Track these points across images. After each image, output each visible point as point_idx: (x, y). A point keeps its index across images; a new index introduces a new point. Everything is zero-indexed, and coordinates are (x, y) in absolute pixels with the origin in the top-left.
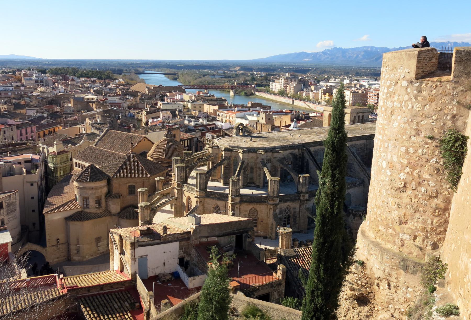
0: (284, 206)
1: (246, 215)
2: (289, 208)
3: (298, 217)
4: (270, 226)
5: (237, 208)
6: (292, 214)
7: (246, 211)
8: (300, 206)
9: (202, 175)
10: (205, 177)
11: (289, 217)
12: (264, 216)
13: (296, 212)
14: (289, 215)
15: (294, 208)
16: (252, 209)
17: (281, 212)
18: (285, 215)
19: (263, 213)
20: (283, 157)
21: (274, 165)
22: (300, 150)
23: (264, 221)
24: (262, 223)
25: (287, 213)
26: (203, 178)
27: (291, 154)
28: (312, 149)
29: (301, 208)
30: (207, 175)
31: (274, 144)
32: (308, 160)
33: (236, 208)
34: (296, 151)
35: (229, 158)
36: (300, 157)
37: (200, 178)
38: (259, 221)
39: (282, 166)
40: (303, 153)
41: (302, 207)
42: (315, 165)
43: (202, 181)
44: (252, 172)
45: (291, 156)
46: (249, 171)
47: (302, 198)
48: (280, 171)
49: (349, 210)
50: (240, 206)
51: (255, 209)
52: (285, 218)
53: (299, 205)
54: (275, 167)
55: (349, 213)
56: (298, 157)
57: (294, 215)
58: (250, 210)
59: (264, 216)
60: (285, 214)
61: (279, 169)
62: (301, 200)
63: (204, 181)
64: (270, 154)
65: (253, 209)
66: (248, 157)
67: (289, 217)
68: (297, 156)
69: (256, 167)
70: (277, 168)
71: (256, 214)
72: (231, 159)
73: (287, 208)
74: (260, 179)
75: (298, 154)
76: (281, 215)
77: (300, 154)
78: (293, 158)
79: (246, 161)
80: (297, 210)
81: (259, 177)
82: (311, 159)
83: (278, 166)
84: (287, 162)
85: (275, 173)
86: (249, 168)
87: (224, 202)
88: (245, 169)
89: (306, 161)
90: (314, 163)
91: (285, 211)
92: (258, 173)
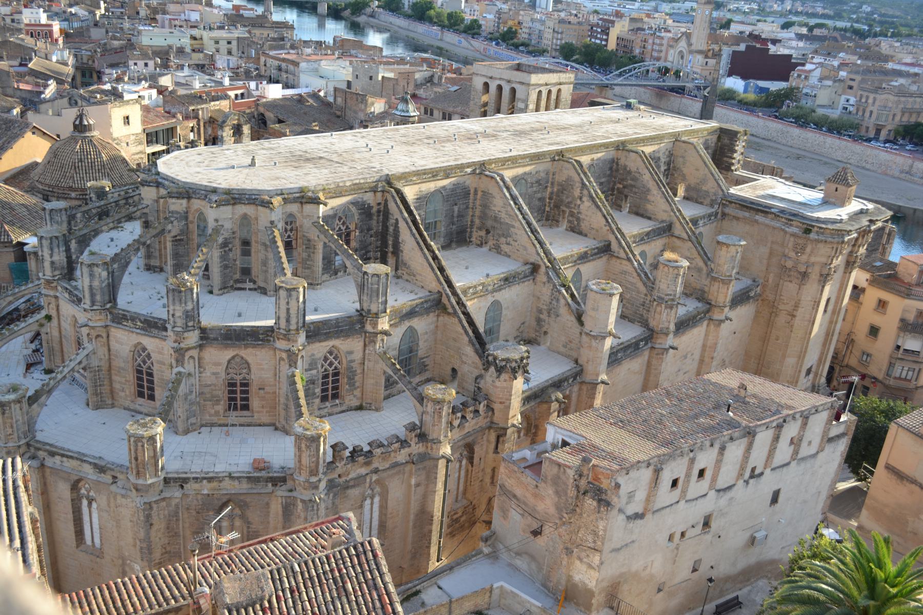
0: (320, 348)
1: (218, 373)
2: (336, 352)
3: (359, 371)
4: (282, 400)
5: (192, 357)
6: (344, 365)
7: (218, 364)
8: (365, 345)
9: (95, 269)
10: (105, 274)
11: (336, 374)
12: (268, 375)
13: (354, 361)
14: (336, 368)
15: (351, 353)
16: (233, 358)
17: (312, 366)
18: (326, 370)
19: (263, 369)
20: (331, 213)
21: (304, 236)
22: (379, 195)
23: (267, 389)
24: (262, 391)
25: (331, 364)
26: (100, 277)
27: (354, 203)
28: (410, 193)
29: (367, 351)
30: (115, 266)
31: (309, 178)
32: (397, 220)
33: (186, 358)
34: (369, 198)
35: (185, 216)
36: (379, 211)
37: (92, 275)
38: (253, 389)
39: (327, 241)
40: (386, 201)
41: (369, 349)
42: (413, 235)
43: (96, 283)
44: (246, 253)
45: (354, 209)
46: (239, 252)
47: (369, 328)
48: (321, 251)
49: (489, 355)
50: (201, 350)
51: (242, 358)
52: (326, 376)
53: (362, 344)
54: (309, 240)
55: (488, 361)
56: (374, 210)
57: (349, 368)
58: (229, 362)
59: (268, 375)
60: (326, 365)
61: (320, 247)
62: (366, 332)
63: (104, 285)
64: (294, 208)
65: (238, 360)
66: (233, 213)
67: (336, 374)
68: (370, 207)
69: (257, 242)
70: (312, 243)
71: (244, 371)
72: (191, 218)
73: (331, 353)
74: (266, 271)
75: (373, 204)
76: (314, 372)
77: (379, 204)
78: (360, 214)
79: (228, 225)
80: (358, 356)
81: (264, 268)
82: (405, 219)
83: (316, 238)
84: (343, 224)
85: (309, 256)
86: (237, 243)
87: (157, 340)
88: (225, 244)
89: (392, 221)
90: (411, 230)
91: (326, 359)
92: (261, 256)
